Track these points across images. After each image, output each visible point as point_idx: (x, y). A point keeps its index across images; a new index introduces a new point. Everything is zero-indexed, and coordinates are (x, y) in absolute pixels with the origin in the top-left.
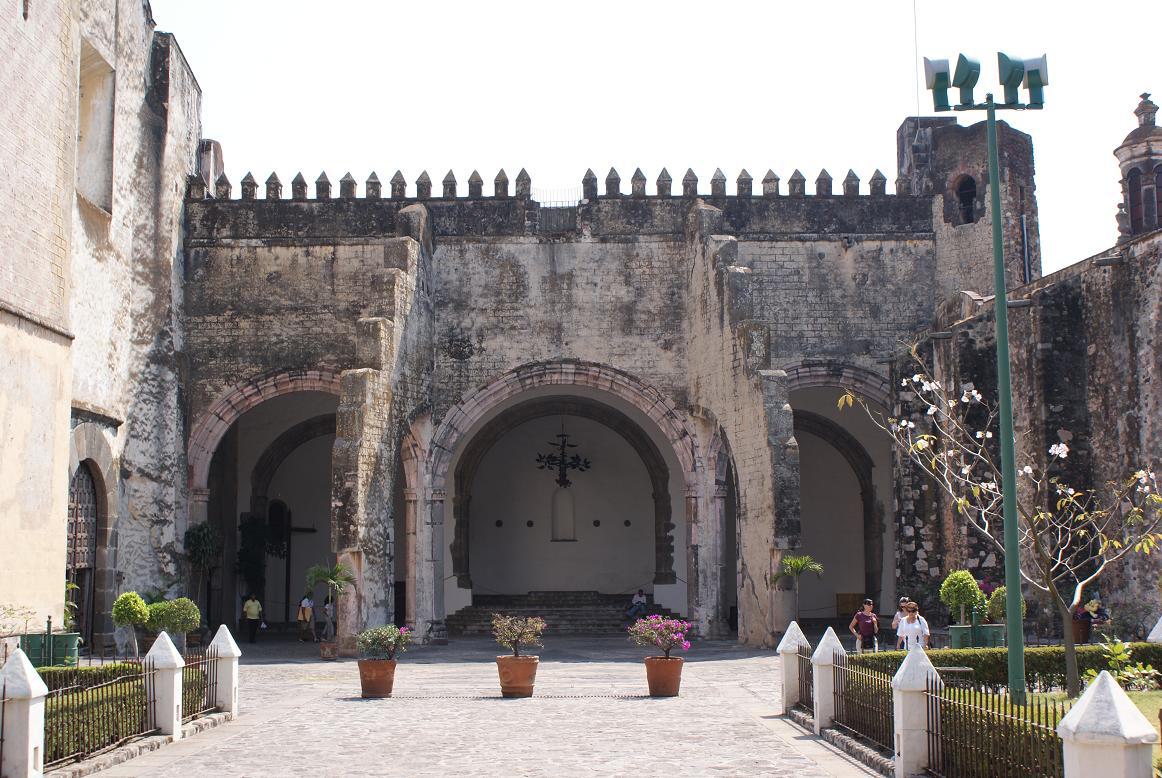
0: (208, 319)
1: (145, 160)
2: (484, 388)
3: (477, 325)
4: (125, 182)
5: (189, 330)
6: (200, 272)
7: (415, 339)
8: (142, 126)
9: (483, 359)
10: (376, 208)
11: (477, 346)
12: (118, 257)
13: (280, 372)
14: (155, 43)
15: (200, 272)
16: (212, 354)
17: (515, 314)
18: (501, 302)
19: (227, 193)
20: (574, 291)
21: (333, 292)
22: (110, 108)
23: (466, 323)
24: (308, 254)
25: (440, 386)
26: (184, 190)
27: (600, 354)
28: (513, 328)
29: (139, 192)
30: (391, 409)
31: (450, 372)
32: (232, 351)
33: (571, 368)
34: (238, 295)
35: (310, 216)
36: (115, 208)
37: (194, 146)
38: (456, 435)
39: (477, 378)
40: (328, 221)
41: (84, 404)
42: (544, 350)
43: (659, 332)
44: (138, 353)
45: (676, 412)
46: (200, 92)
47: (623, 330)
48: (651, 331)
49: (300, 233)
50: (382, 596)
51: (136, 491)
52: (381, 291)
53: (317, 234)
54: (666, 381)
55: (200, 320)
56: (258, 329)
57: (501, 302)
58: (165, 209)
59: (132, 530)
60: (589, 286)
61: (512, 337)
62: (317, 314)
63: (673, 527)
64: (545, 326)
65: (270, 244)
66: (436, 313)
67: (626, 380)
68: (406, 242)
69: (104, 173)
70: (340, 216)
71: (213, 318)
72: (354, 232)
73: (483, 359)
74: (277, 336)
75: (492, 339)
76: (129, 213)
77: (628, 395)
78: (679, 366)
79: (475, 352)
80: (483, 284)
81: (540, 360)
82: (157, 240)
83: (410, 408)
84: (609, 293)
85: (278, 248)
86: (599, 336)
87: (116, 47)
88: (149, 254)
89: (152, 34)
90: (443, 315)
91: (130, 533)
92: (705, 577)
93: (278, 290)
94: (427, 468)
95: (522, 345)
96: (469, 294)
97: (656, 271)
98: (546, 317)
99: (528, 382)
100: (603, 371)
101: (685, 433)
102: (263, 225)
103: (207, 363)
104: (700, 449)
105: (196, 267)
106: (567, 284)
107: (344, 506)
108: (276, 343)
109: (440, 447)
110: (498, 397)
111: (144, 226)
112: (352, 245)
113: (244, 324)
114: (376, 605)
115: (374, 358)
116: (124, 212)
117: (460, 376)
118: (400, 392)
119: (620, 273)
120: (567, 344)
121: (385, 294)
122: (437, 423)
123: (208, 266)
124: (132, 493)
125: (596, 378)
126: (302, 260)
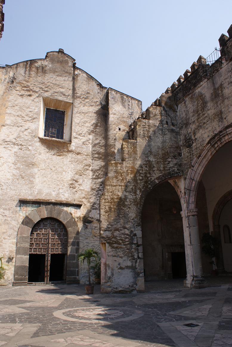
1: (99, 124)
2: (200, 156)
8: (98, 115)
22: (72, 113)
28: (204, 123)
29: (95, 134)
36: (73, 140)
38: (194, 182)
41: (49, 200)
44: (96, 182)
50: (129, 264)
51: (95, 227)
57: (199, 114)
59: (94, 240)
61: (204, 128)
64: (215, 116)
80: (193, 111)
81: (216, 133)
82: (107, 146)
90: (182, 132)
91: (93, 241)
95: (208, 130)
99: (216, 146)
106: (221, 90)
111: (99, 143)
114: (121, 268)
116: (83, 140)
117: (190, 155)
122: (185, 179)
124: (94, 228)
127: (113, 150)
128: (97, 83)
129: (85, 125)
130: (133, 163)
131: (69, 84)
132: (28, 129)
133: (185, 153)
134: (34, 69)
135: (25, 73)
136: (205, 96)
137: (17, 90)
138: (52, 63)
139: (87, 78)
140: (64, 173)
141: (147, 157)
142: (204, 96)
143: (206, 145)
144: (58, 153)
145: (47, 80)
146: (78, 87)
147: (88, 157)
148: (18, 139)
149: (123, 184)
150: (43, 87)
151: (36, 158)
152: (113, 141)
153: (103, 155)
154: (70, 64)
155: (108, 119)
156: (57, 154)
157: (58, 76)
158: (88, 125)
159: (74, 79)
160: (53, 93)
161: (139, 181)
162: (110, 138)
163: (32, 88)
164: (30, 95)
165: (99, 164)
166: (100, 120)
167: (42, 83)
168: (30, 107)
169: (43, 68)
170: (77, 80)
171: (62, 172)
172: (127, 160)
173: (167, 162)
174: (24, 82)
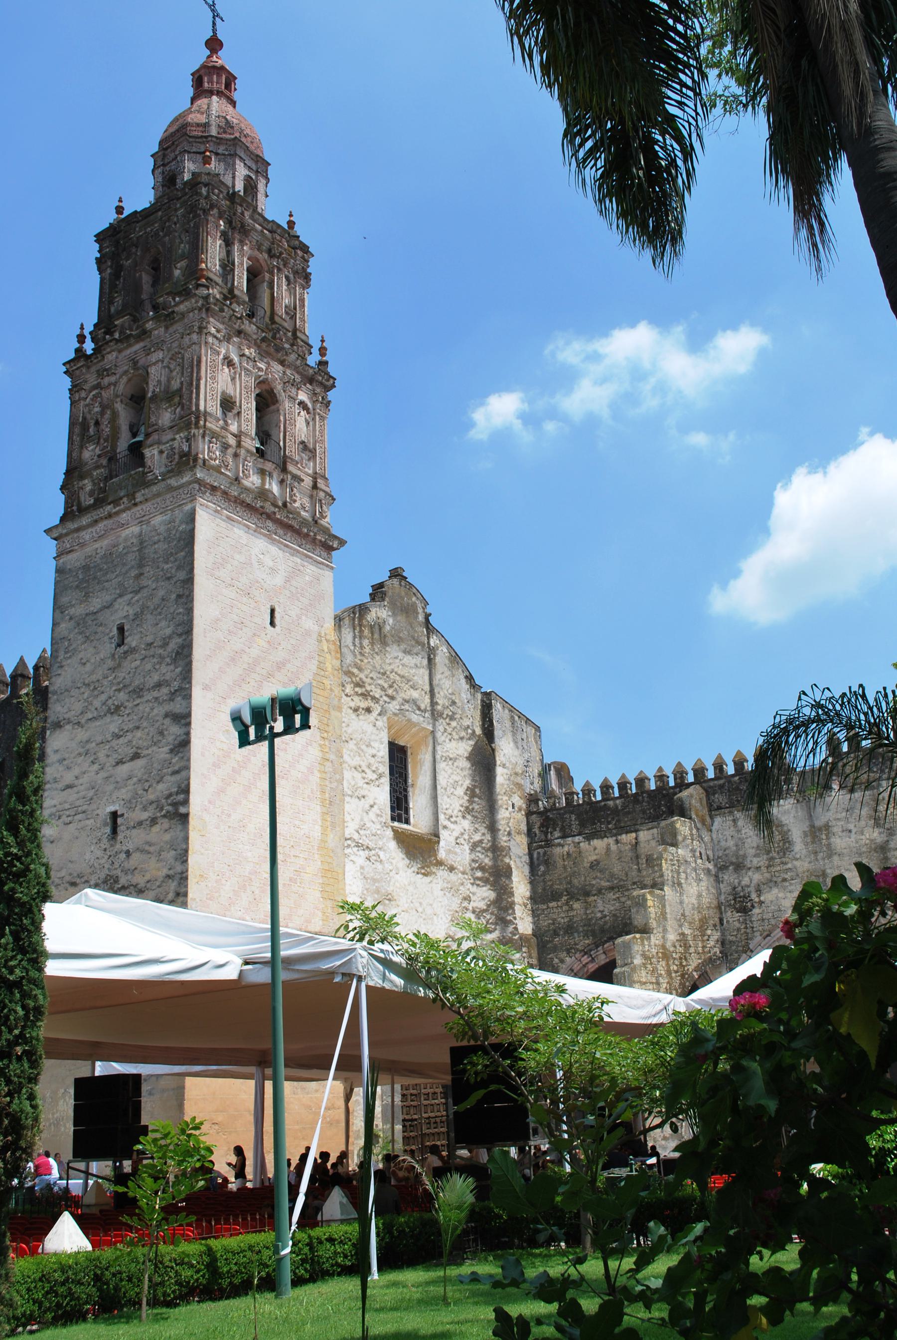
0: (551, 905)
1: (477, 791)
2: (768, 935)
3: (755, 882)
4: (456, 812)
5: (538, 916)
6: (542, 868)
7: (695, 902)
10: (664, 796)
12: (452, 869)
13: (606, 942)
14: (482, 701)
15: (542, 868)
16: (556, 933)
18: (772, 859)
19: (554, 804)
20: (832, 840)
21: (639, 870)
23: (745, 881)
24: (617, 842)
25: (731, 938)
26: (524, 806)
28: (785, 880)
29: (473, 816)
30: (668, 965)
31: (737, 925)
32: (570, 929)
34: (570, 883)
35: (615, 811)
36: (443, 834)
37: (536, 769)
39: (761, 928)
40: (629, 813)
46: (538, 729)
49: (610, 826)
52: (653, 867)
53: (622, 825)
55: (545, 907)
56: (586, 909)
57: (772, 859)
58: (502, 825)
60: (844, 834)
61: (785, 888)
62: (628, 890)
65: (589, 838)
66: (720, 876)
68: (674, 822)
69: (431, 808)
70: (638, 808)
71: (553, 904)
72: (649, 818)
74: (602, 912)
75: (769, 892)
76: (462, 834)
79: (756, 905)
80: (755, 845)
82: (495, 849)
83: (694, 962)
84: (863, 837)
85: (595, 841)
87: (433, 714)
88: (487, 861)
89: (479, 696)
90: (726, 877)
93: (599, 874)
96: (744, 856)
98: (811, 867)
102: (582, 824)
103: (553, 941)
105: (539, 865)
108: (601, 918)
111: (481, 841)
112: (649, 829)
113: (576, 905)
115: (645, 924)
116: (456, 834)
117: (746, 928)
118: (681, 950)
121: (656, 868)
123: (547, 863)
126: (614, 847)
127: (507, 860)
128: (468, 674)
129: (456, 793)
130: (663, 937)
131: (421, 676)
132: (375, 803)
133: (731, 920)
134: (366, 632)
135: (355, 645)
136: (789, 830)
137: (347, 695)
138: (394, 615)
139: (449, 659)
140: (435, 917)
141: (681, 926)
142: (785, 828)
144: (423, 868)
145: (390, 664)
146: (438, 685)
147: (466, 877)
148: (362, 832)
149: (654, 981)
150: (386, 685)
151: (393, 880)
152: (505, 838)
153: (491, 874)
154: (421, 618)
155: (495, 777)
156: (423, 871)
157: (405, 652)
158: (460, 791)
159: (430, 660)
160: (403, 704)
161: (673, 975)
162: (499, 830)
163: (368, 688)
164: (368, 710)
165: (483, 895)
166: (477, 778)
167: (384, 674)
168: (372, 743)
169: (380, 629)
170: (435, 664)
171: (432, 919)
172: (655, 931)
173: (706, 937)
174: (355, 671)
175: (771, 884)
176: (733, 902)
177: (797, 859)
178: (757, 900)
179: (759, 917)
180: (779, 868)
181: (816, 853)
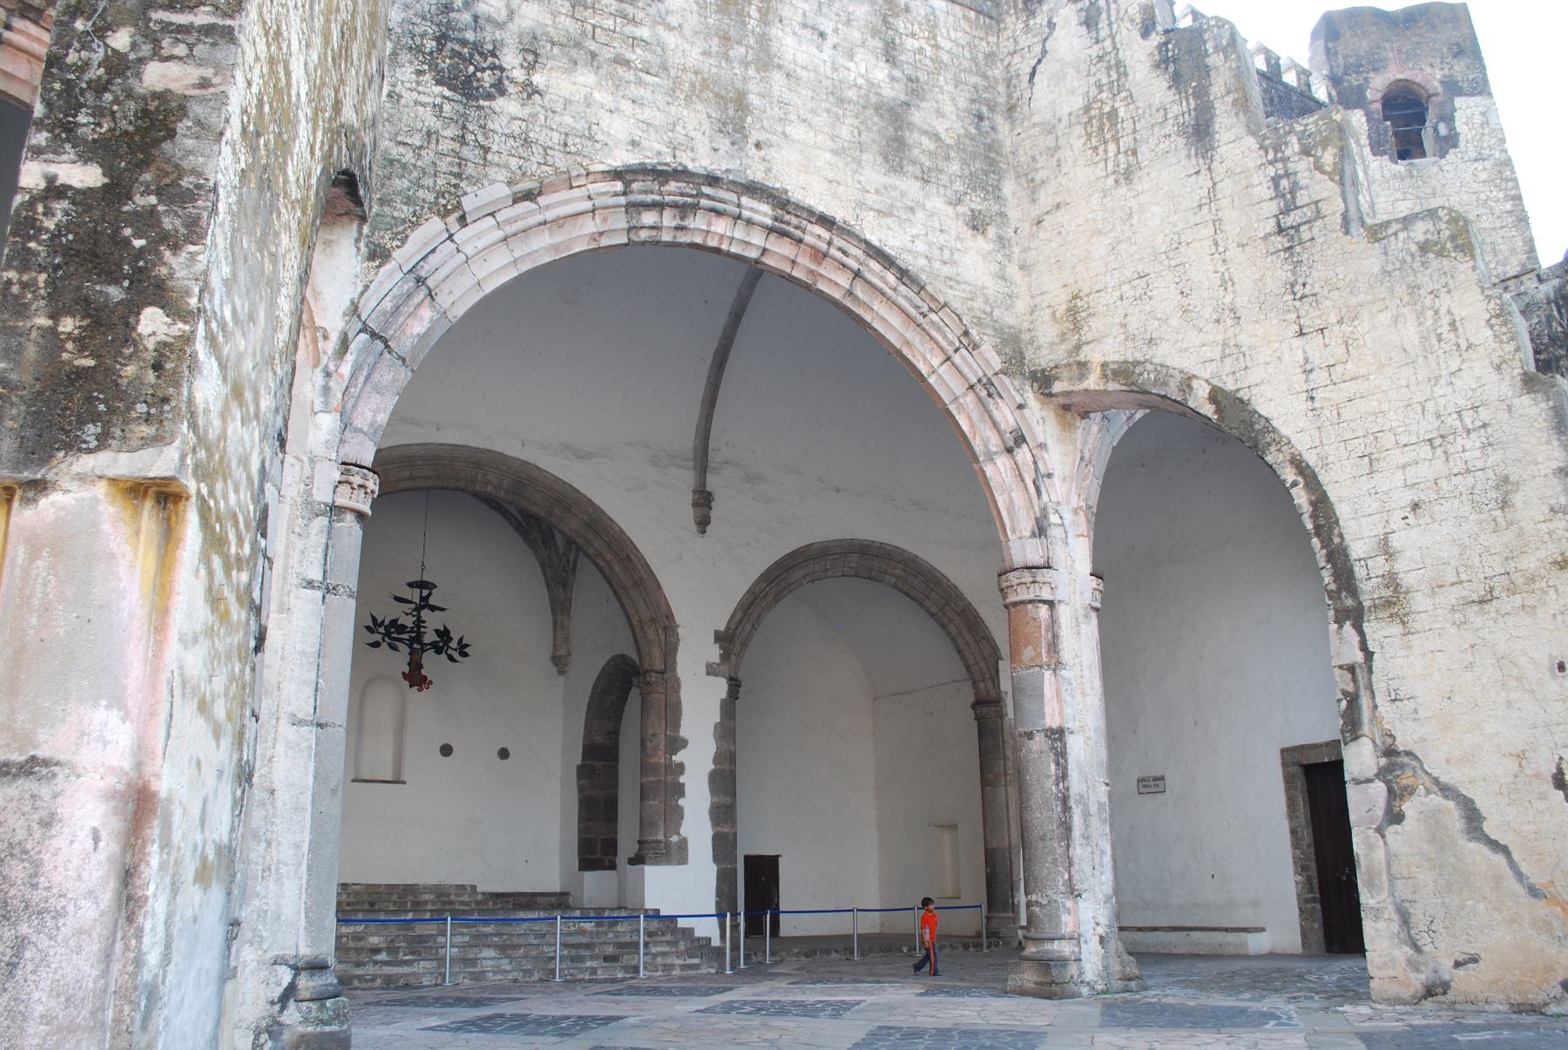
2: (529, 196)
9: (534, 116)
11: (519, 74)
17: (629, 29)
25: (395, 151)
27: (835, 196)
31: (431, 121)
33: (762, 212)
38: (426, 314)
39: (514, 162)
42: (702, 145)
43: (958, 186)
45: (1007, 384)
47: (886, 159)
48: (944, 179)
54: (978, 304)
60: (807, 33)
61: (619, 84)
63: (684, 743)
67: (891, 278)
73: (534, 116)
77: (888, 323)
78: (1003, 278)
79: (511, 89)
81: (690, 166)
84: (851, 65)
86: (835, 152)
92: (1086, 815)
94: (326, 390)
95: (646, 114)
97: (945, 58)
98: (710, 66)
99: (649, 218)
100: (838, 242)
101: (1020, 439)
104: (1056, 480)
106: (759, 10)
107: (115, 191)
109: (374, 335)
110: (559, 237)
117: (462, 140)
119: (875, 32)
120: (758, 146)
122: (378, 255)
125: (820, 256)
133: (408, 97)
143: (603, 172)
175: (580, 56)
176: (430, 45)
177: (671, 29)
178: (519, 74)
179: (516, 127)
180: (609, 23)
181: (726, 39)
